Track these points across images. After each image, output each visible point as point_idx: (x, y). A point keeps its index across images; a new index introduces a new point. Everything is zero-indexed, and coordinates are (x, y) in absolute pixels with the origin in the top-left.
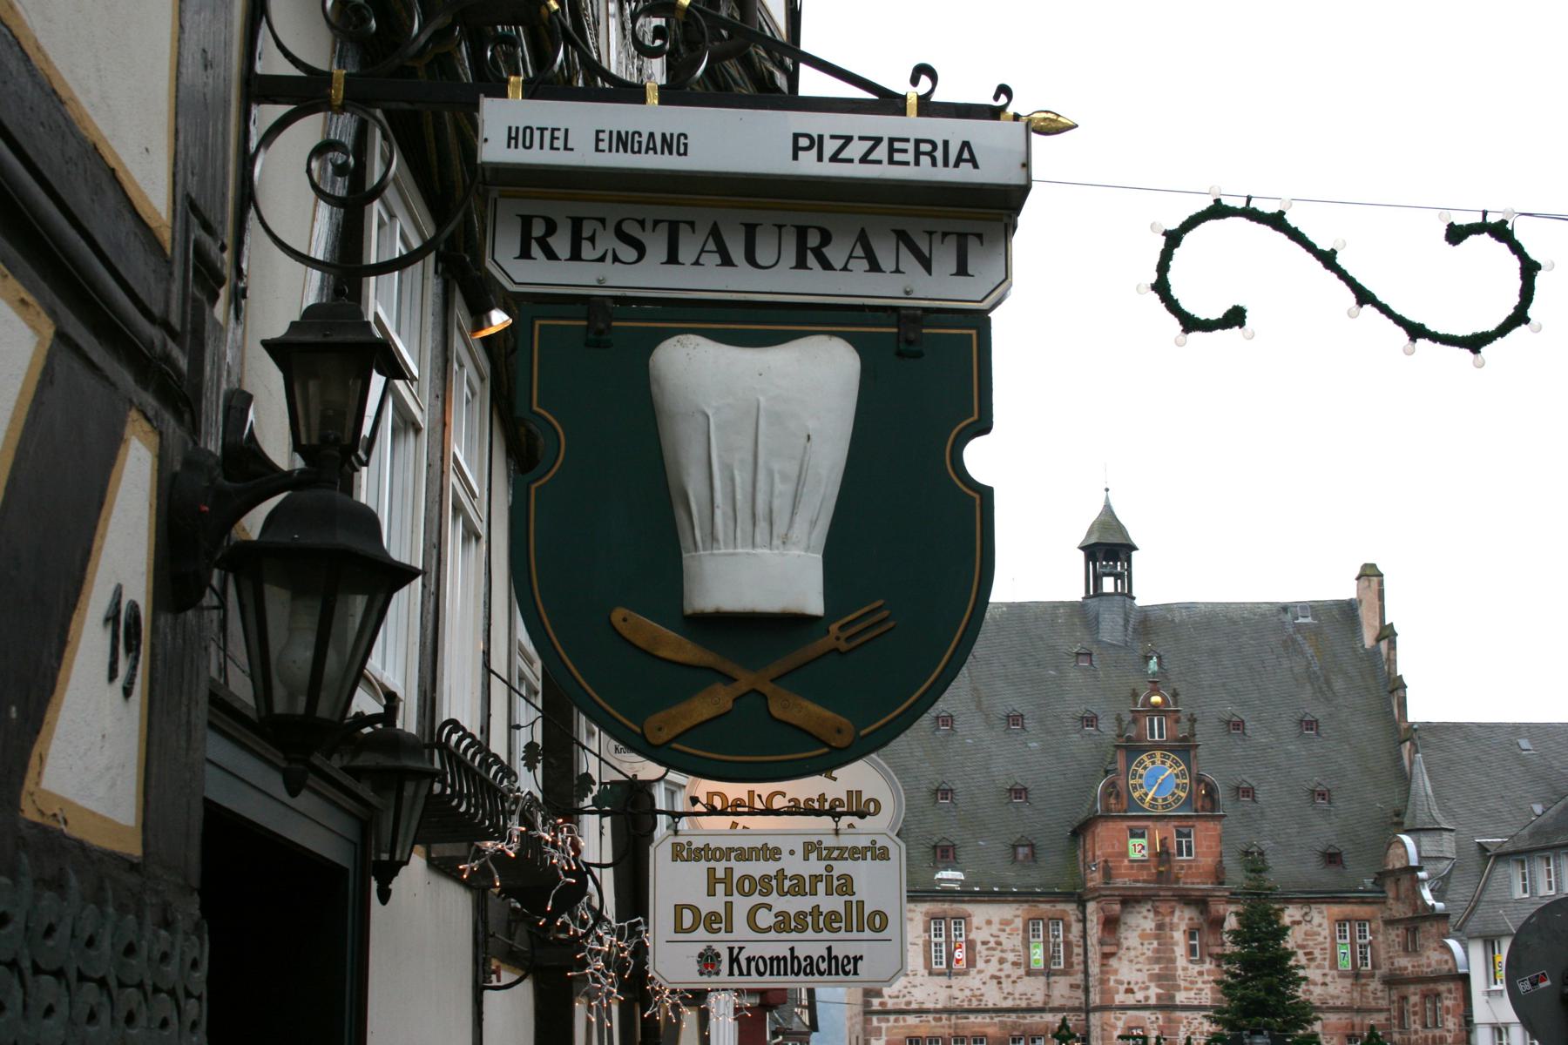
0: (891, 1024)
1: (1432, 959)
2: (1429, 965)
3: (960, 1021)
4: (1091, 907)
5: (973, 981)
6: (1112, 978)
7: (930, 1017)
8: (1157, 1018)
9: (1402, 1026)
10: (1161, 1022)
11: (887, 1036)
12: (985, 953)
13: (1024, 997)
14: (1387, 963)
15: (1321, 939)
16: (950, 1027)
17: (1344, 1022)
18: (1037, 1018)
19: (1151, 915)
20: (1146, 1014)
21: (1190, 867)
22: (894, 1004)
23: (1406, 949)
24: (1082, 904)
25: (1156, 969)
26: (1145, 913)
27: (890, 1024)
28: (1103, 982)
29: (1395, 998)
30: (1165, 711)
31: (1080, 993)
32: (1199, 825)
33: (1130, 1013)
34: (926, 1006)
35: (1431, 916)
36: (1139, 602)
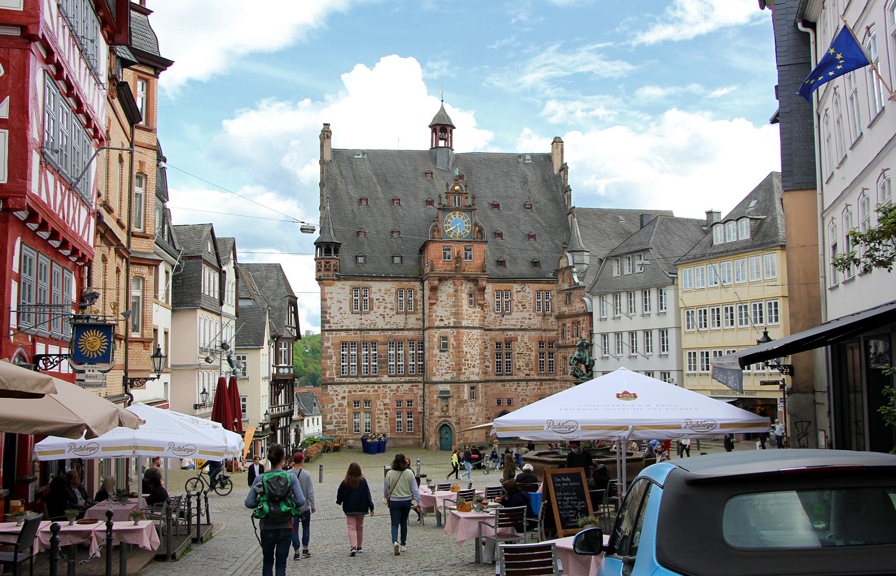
0: (334, 335)
1: (577, 307)
2: (576, 310)
4: (426, 283)
5: (372, 316)
6: (434, 314)
7: (352, 332)
9: (563, 337)
12: (377, 304)
14: (558, 309)
15: (529, 299)
16: (361, 337)
17: (538, 335)
18: (401, 333)
19: (452, 286)
21: (470, 264)
23: (566, 303)
24: (422, 282)
25: (454, 310)
26: (449, 285)
28: (429, 316)
29: (560, 325)
30: (460, 193)
31: (421, 322)
32: (476, 245)
33: (441, 330)
34: (349, 328)
35: (578, 287)
36: (455, 152)
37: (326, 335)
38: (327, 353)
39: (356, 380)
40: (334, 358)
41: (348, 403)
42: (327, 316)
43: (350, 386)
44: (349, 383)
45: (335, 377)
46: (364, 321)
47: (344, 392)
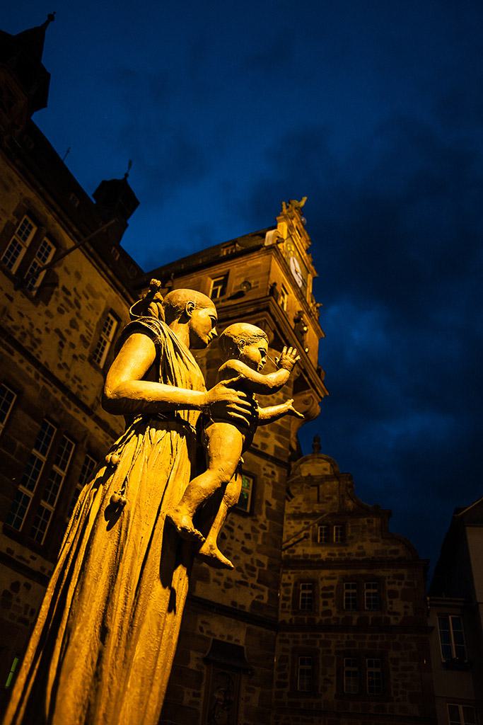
8: (273, 473)
10: (277, 479)
12: (62, 300)
13: (77, 381)
20: (263, 462)
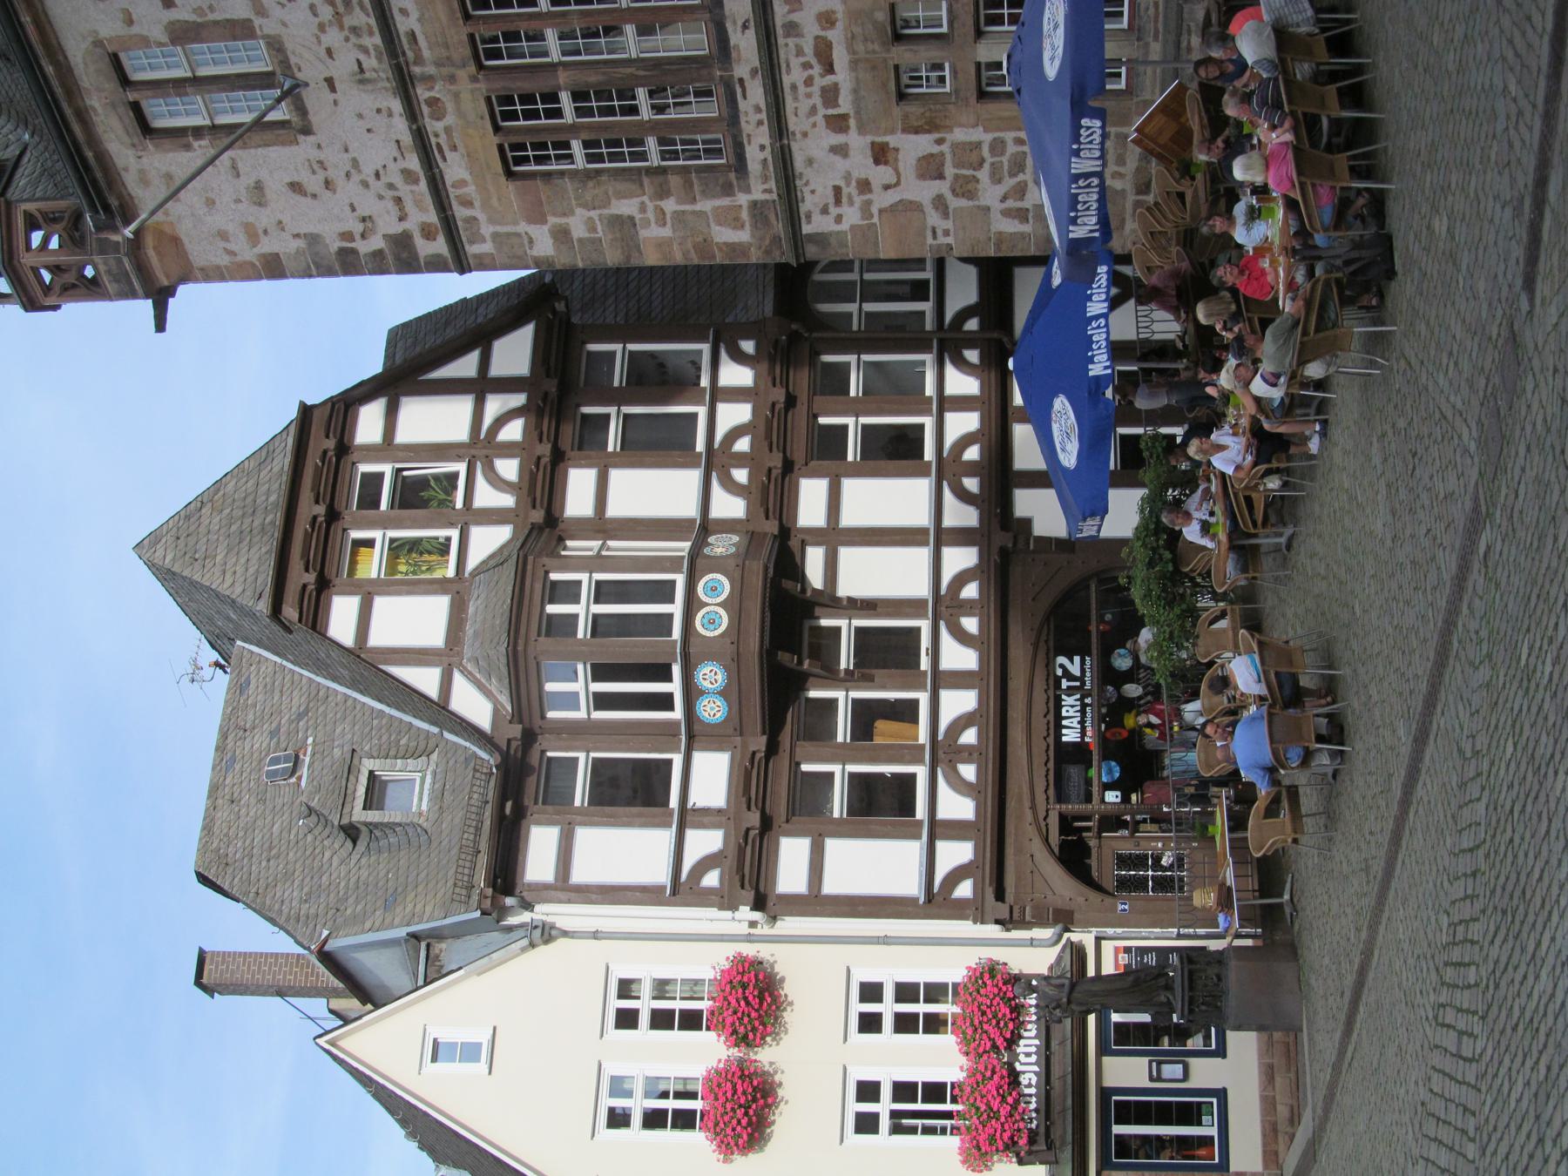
3: (426, 53)
7: (433, 126)
11: (516, 223)
22: (422, 209)
27: (482, 217)
34: (407, 139)
37: (486, 248)
38: (593, 241)
39: (755, 96)
40: (626, 207)
41: (917, 131)
42: (364, 247)
43: (793, 123)
44: (779, 128)
45: (743, 199)
46: (343, 66)
47: (841, 151)
